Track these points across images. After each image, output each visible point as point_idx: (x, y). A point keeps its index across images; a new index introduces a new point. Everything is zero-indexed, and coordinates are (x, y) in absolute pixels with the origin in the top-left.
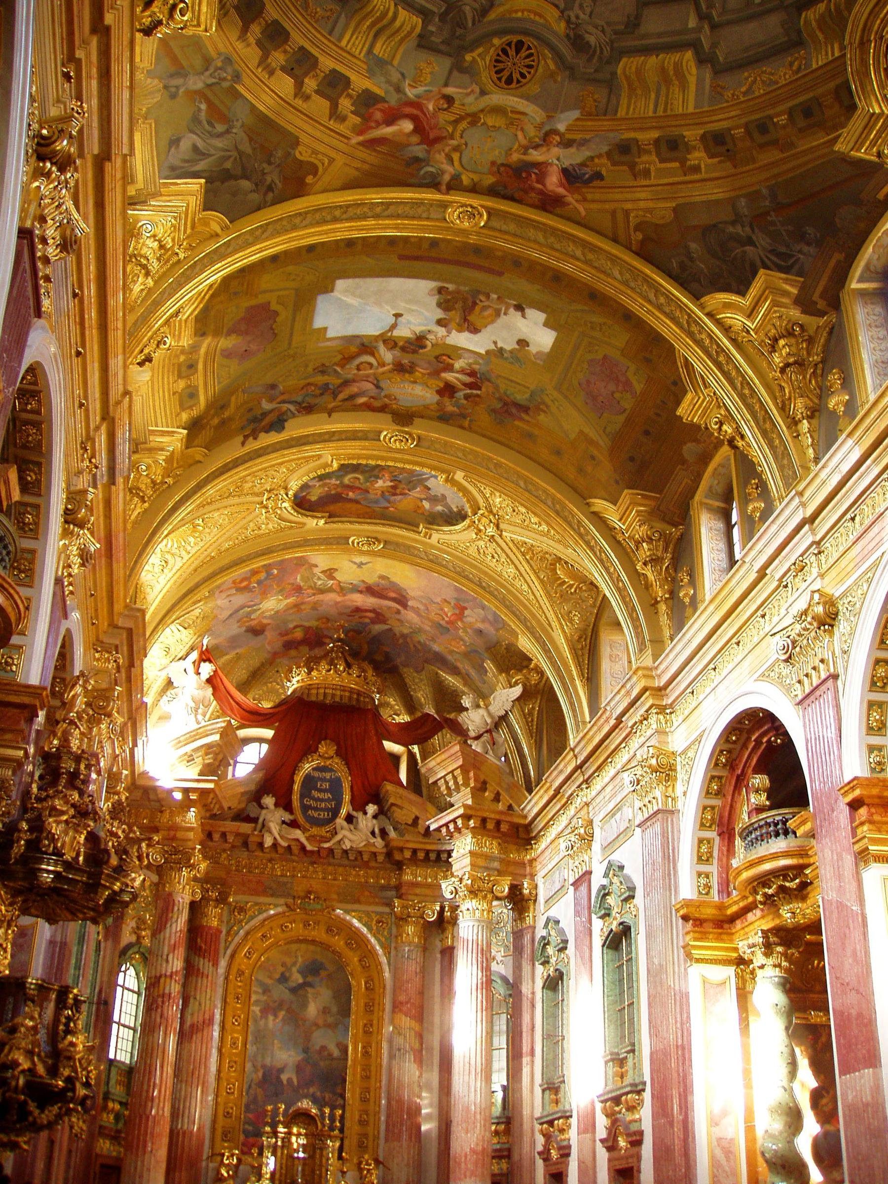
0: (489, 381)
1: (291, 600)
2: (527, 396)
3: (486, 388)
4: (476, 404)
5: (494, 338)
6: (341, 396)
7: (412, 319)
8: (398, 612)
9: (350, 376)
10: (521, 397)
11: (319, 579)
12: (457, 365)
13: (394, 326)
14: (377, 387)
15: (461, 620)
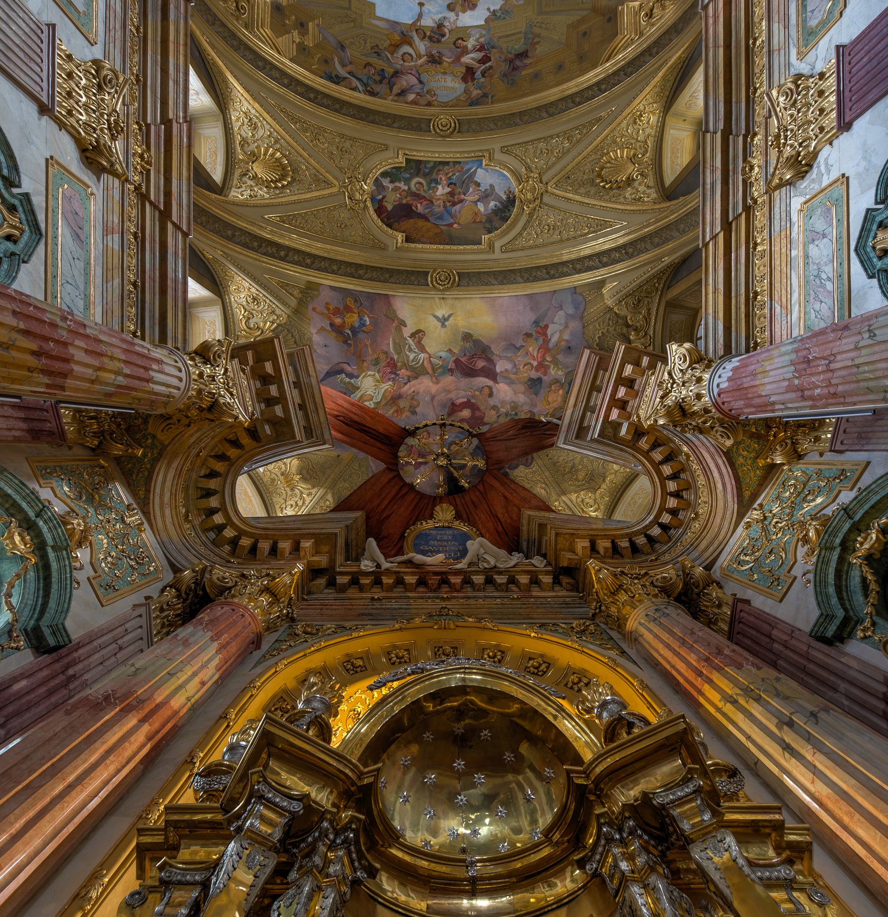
0: (493, 47)
1: (386, 386)
2: (522, 41)
3: (495, 55)
4: (491, 76)
5: (486, 7)
6: (396, 90)
7: (430, 8)
8: (491, 395)
9: (398, 66)
10: (519, 46)
11: (410, 350)
12: (471, 43)
13: (420, 16)
14: (421, 82)
15: (548, 350)
